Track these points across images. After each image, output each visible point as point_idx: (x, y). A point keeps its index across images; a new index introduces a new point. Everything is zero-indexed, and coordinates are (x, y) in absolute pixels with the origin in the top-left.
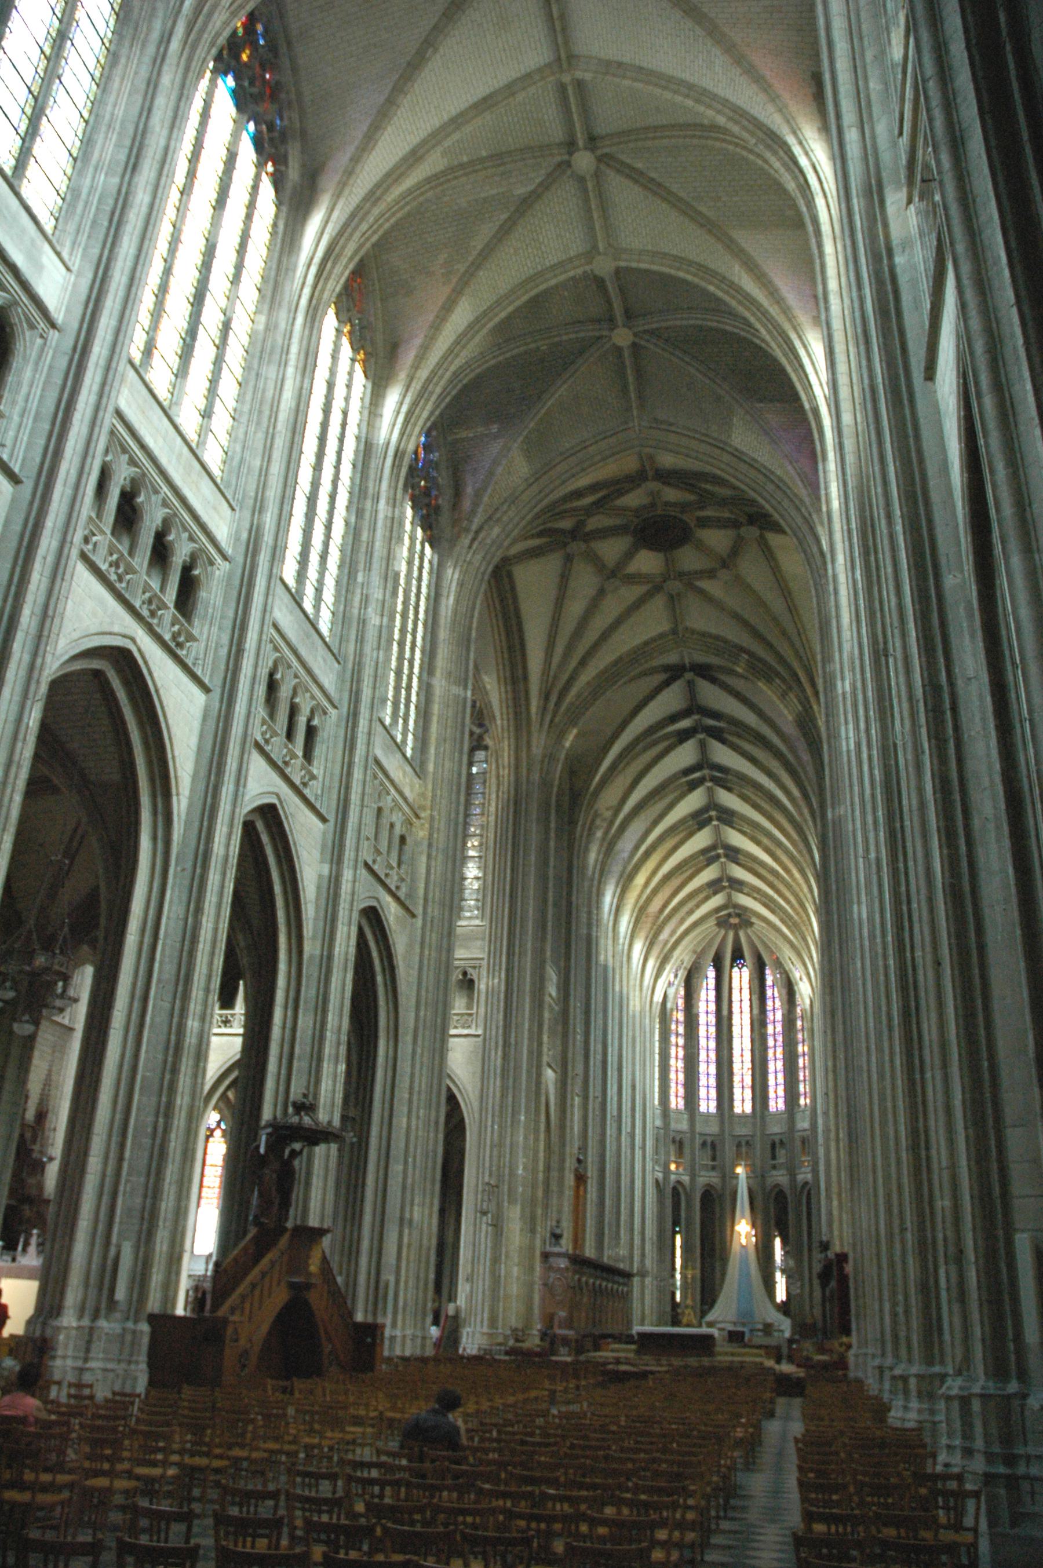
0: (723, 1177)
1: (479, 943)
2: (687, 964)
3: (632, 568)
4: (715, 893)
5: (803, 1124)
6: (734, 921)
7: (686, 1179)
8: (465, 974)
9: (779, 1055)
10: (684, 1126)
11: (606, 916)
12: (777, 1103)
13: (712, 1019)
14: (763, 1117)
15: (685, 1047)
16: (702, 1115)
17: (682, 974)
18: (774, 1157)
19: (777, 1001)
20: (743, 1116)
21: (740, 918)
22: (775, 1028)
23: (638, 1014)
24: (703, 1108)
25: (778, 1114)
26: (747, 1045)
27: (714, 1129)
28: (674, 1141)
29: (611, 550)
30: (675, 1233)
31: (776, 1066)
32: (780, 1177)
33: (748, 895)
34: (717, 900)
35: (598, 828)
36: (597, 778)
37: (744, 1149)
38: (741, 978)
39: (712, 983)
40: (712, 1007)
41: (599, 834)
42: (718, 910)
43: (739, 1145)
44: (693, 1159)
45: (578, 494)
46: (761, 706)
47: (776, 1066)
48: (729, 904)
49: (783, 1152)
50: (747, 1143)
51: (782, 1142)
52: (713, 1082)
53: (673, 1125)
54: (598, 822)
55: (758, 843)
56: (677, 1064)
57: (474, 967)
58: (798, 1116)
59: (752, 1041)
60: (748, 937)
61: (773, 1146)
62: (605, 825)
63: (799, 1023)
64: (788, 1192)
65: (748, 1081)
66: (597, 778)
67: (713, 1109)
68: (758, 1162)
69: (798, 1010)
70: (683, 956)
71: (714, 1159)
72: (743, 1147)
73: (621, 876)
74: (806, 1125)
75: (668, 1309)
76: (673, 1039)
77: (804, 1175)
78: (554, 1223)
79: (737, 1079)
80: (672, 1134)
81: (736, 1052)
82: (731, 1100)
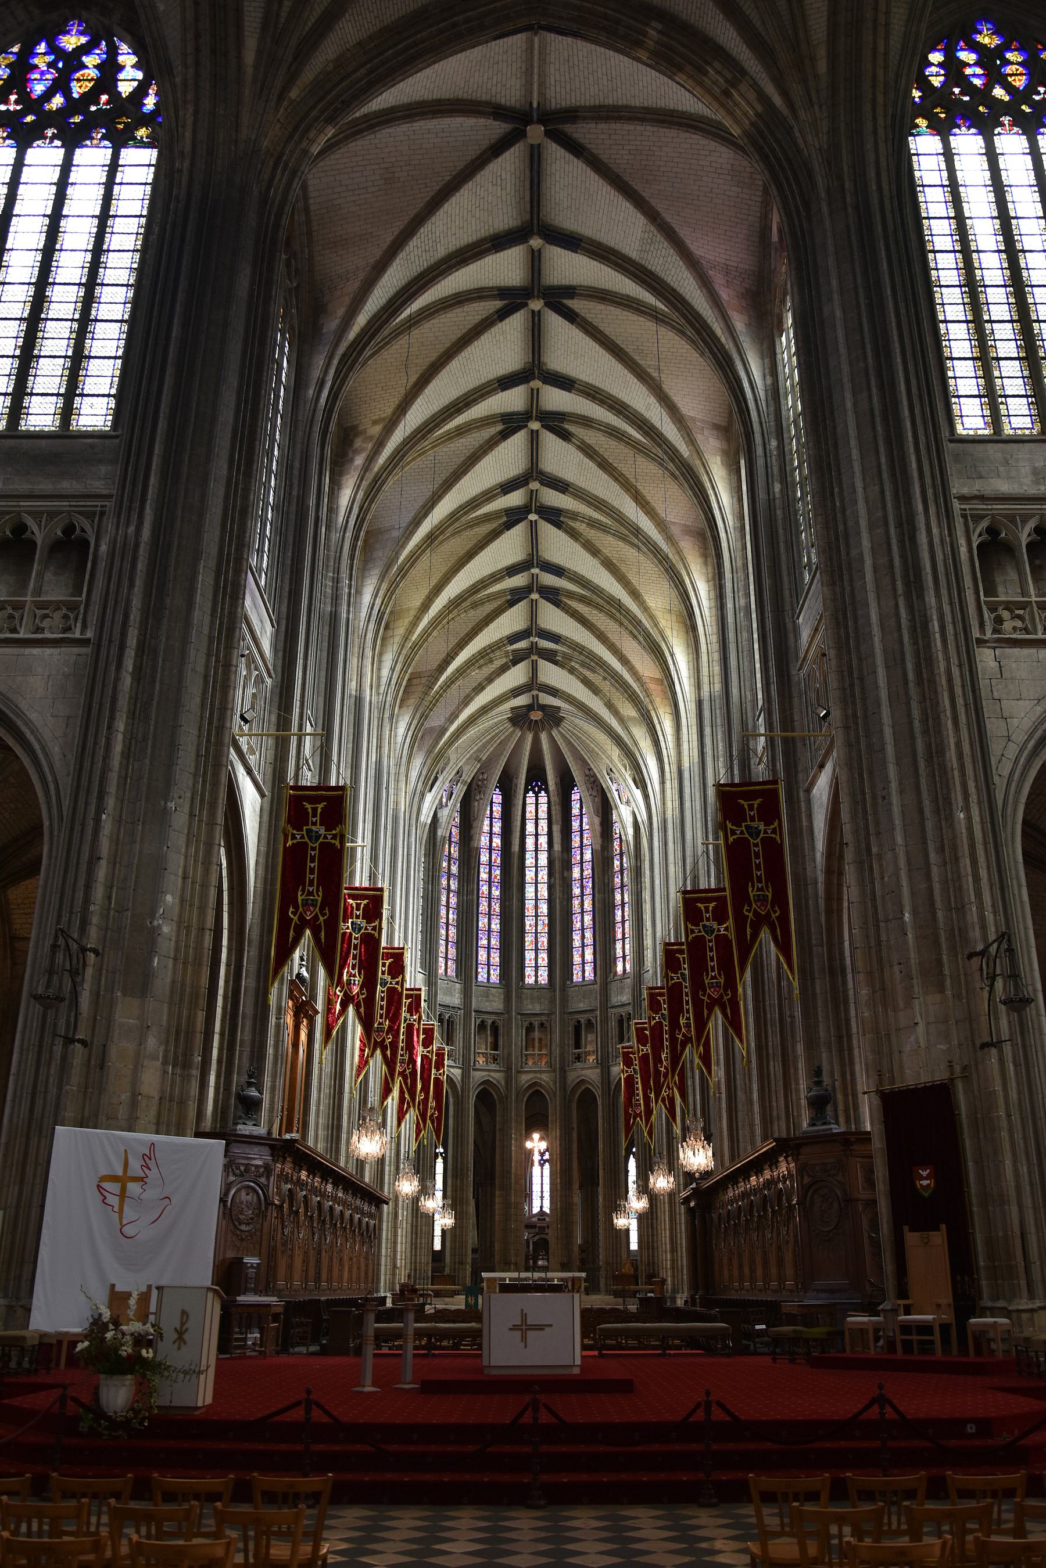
0: (508, 1070)
1: (103, 469)
2: (467, 777)
4: (515, 662)
5: (622, 997)
6: (536, 716)
8: (69, 529)
9: (588, 905)
10: (456, 1000)
14: (564, 988)
15: (459, 893)
17: (460, 791)
18: (578, 1045)
20: (537, 987)
22: (581, 871)
24: (482, 976)
25: (584, 984)
26: (544, 891)
27: (496, 1004)
30: (436, 1156)
31: (583, 920)
32: (589, 1072)
33: (562, 667)
34: (517, 676)
35: (357, 452)
36: (361, 320)
37: (536, 1034)
38: (536, 808)
39: (497, 809)
40: (497, 841)
41: (359, 461)
42: (516, 692)
43: (530, 1029)
44: (467, 1047)
46: (654, 202)
47: (583, 920)
48: (532, 685)
49: (591, 1037)
50: (542, 1025)
52: (495, 942)
53: (441, 998)
54: (358, 443)
55: (593, 550)
56: (448, 915)
57: (89, 515)
58: (614, 987)
60: (553, 741)
62: (370, 446)
63: (617, 863)
64: (598, 1093)
65: (544, 940)
66: (361, 320)
67: (495, 976)
68: (557, 1052)
69: (616, 844)
71: (495, 1047)
74: (625, 998)
75: (425, 1259)
76: (444, 882)
78: (244, 1078)
79: (529, 939)
81: (529, 904)
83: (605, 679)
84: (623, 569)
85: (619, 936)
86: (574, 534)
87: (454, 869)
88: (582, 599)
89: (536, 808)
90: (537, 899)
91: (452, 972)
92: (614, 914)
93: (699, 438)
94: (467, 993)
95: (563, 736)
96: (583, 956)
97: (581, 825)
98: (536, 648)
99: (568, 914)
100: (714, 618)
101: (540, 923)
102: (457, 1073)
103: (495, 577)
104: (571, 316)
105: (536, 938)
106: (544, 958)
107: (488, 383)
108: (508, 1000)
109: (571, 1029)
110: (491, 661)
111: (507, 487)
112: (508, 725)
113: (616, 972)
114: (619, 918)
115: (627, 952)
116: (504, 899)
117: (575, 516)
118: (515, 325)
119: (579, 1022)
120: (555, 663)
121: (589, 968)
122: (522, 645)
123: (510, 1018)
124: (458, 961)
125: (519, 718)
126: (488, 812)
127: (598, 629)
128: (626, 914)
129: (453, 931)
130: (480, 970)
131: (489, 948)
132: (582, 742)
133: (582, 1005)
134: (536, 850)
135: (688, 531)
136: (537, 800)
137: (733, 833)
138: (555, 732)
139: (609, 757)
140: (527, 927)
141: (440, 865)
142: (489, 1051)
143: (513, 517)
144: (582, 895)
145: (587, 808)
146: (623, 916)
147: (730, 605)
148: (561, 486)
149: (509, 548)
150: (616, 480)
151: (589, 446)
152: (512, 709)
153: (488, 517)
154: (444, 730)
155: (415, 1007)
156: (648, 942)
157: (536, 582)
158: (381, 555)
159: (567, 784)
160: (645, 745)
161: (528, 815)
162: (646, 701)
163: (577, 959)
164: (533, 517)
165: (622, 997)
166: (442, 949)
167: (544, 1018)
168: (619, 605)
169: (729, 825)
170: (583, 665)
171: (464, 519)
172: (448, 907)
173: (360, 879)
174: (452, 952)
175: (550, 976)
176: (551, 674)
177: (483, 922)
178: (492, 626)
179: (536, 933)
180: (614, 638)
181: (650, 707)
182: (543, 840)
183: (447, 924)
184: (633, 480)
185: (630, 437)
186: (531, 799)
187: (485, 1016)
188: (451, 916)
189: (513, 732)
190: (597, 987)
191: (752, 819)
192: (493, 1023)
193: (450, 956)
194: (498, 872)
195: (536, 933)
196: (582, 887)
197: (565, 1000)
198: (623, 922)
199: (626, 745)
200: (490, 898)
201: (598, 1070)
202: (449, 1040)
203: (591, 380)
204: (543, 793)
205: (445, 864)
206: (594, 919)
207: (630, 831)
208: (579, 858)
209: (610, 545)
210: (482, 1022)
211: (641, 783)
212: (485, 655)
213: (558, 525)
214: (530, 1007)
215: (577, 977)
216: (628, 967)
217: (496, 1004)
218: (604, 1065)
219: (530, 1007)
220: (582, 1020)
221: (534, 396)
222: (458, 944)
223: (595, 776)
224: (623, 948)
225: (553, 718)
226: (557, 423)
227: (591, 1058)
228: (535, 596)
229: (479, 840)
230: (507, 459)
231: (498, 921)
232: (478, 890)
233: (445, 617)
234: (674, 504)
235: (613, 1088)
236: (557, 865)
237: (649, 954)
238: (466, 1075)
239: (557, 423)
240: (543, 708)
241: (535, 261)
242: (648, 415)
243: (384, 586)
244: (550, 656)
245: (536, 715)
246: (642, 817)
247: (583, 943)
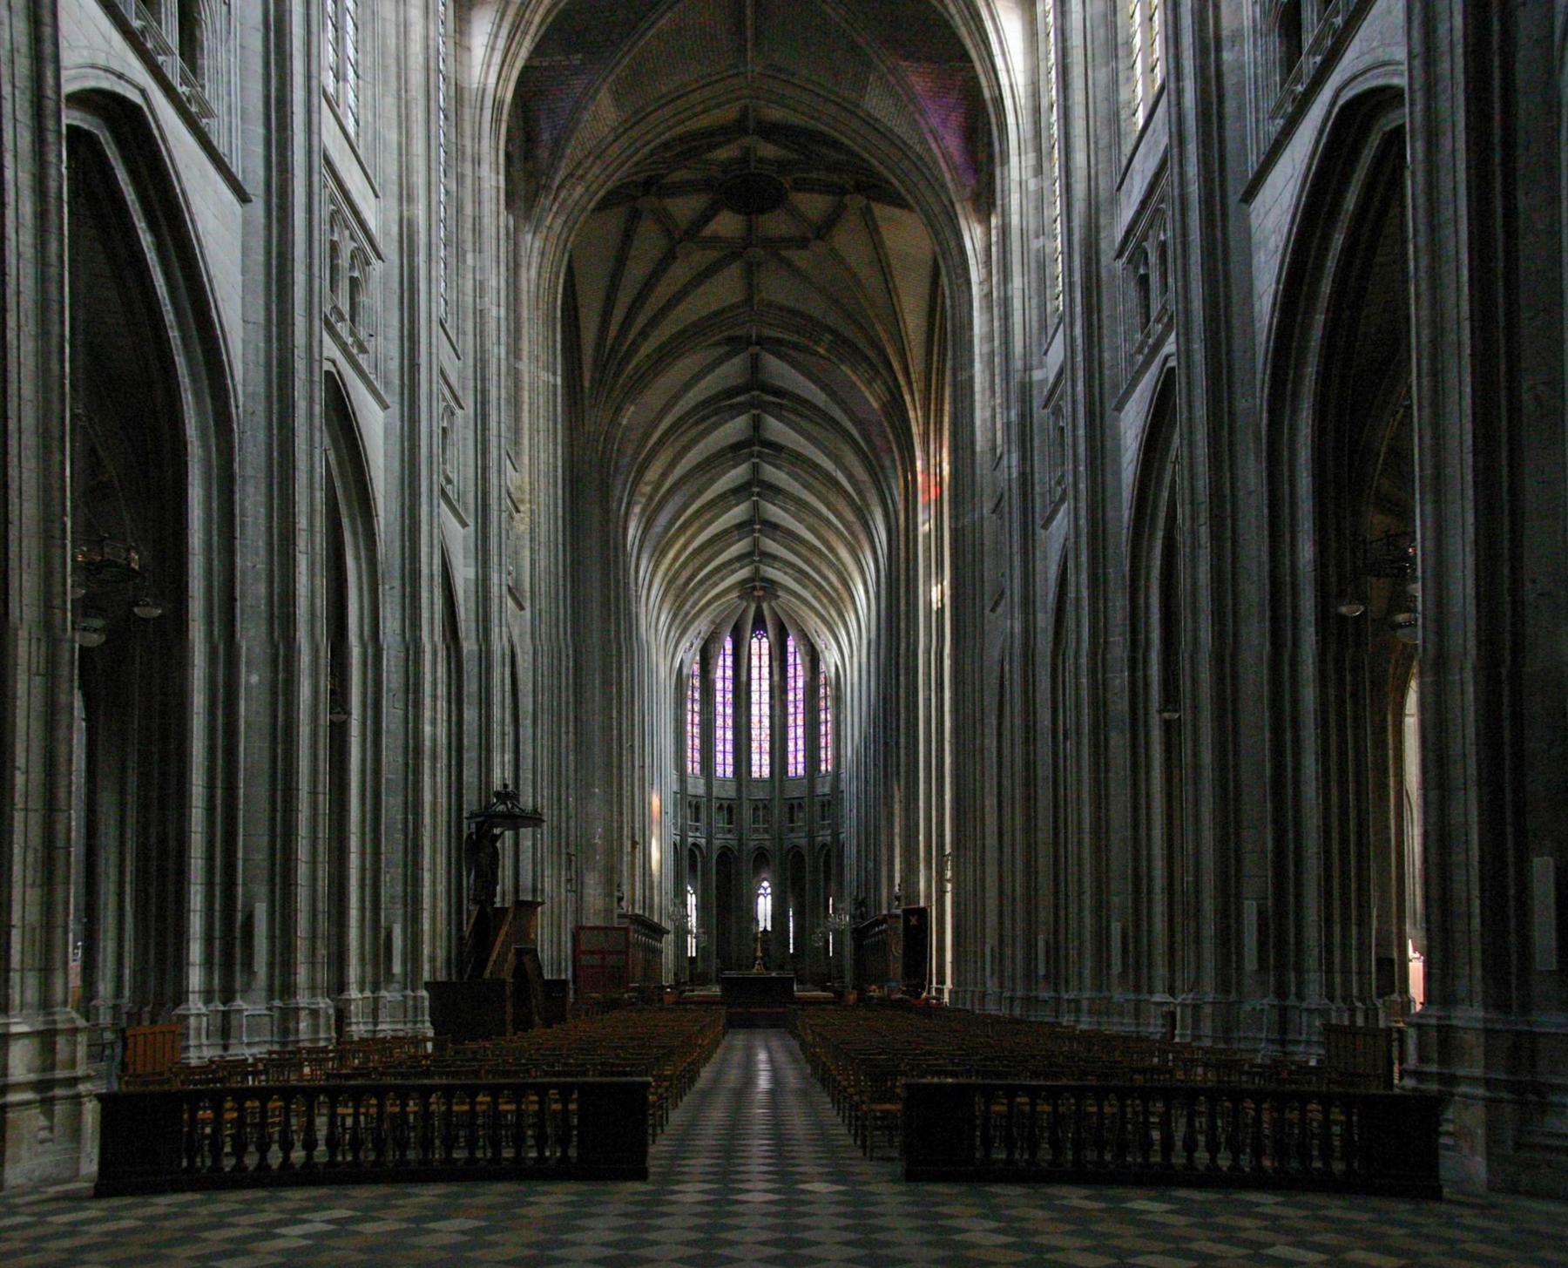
0: (740, 840)
3: (708, 231)
10: (701, 791)
13: (729, 685)
15: (701, 713)
16: (718, 779)
17: (698, 644)
18: (792, 821)
20: (761, 780)
21: (771, 587)
26: (766, 710)
27: (732, 793)
29: (684, 208)
40: (729, 673)
43: (756, 809)
44: (709, 824)
45: (666, 146)
52: (729, 747)
53: (691, 790)
56: (693, 731)
61: (792, 808)
64: (805, 852)
67: (729, 771)
70: (702, 626)
71: (730, 822)
77: (824, 836)
81: (755, 719)
82: (750, 765)
87: (697, 695)
94: (709, 785)
106: (766, 759)
124: (702, 763)
129: (697, 741)
157: (756, 524)
174: (697, 756)
177: (719, 733)
197: (782, 791)
217: (732, 793)
222: (702, 751)
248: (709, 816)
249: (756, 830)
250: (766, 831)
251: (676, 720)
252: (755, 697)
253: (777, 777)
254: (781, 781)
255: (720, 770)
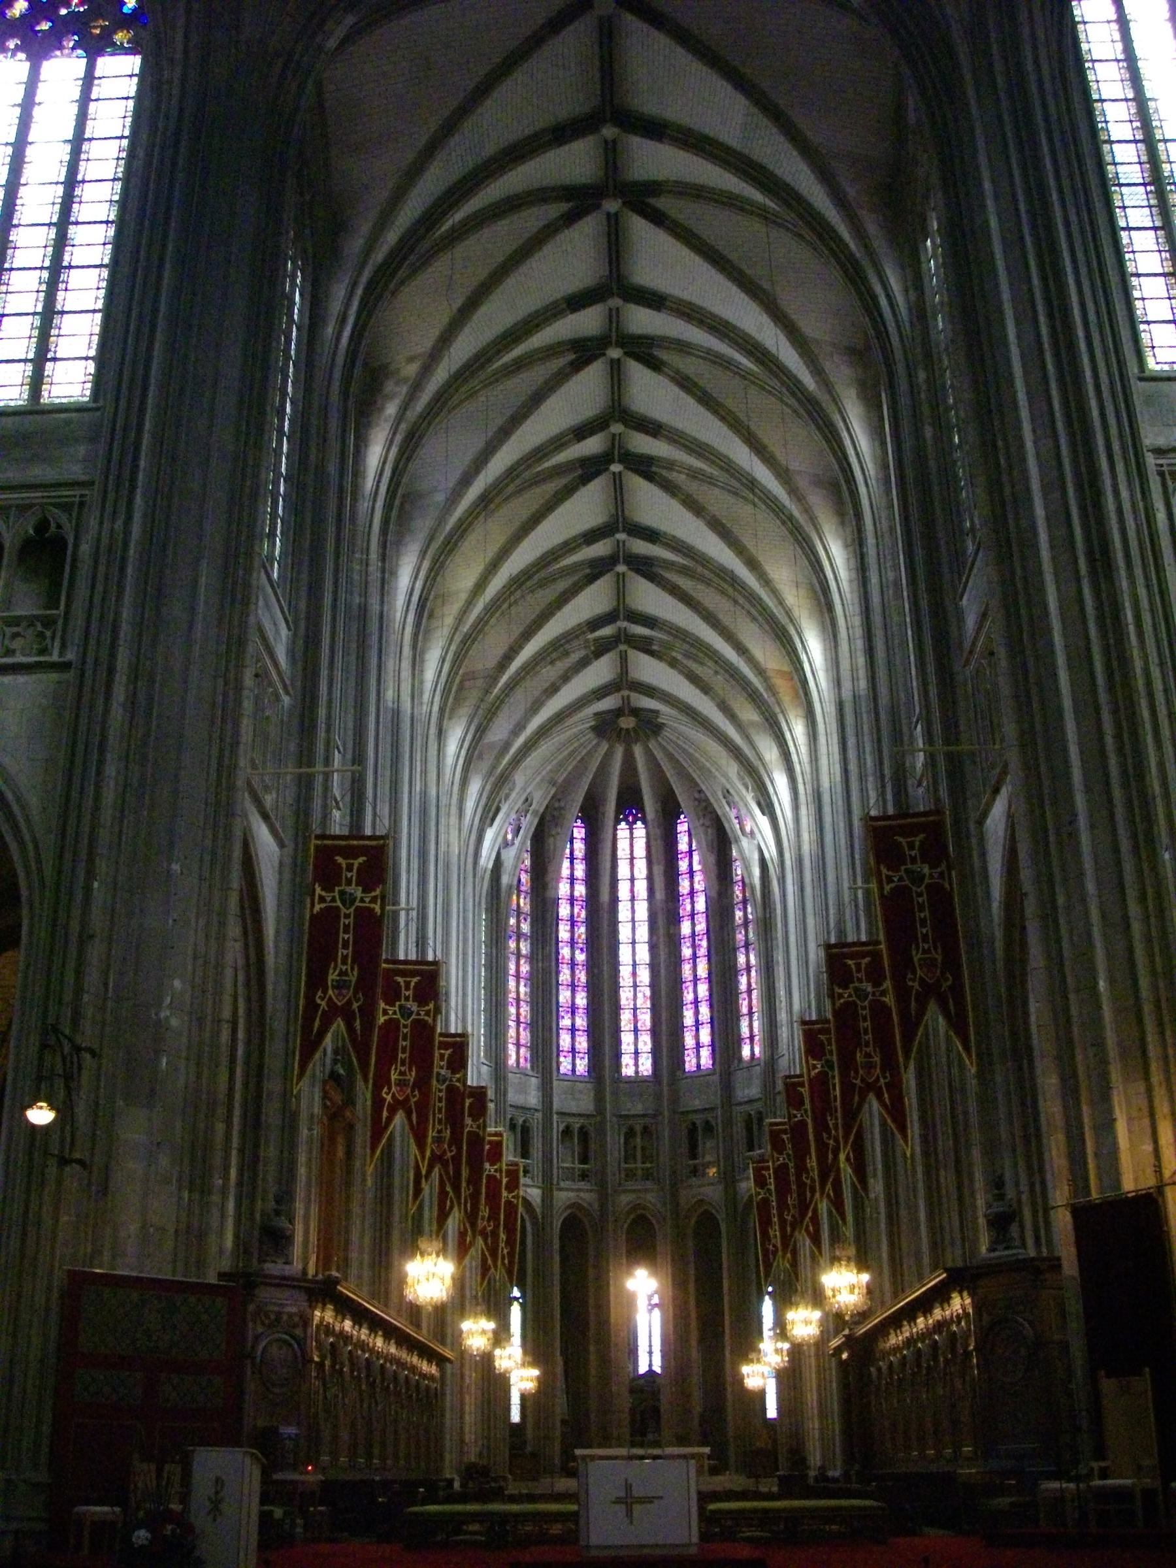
4: (598, 654)
5: (749, 1089)
6: (627, 723)
7: (534, 1194)
9: (702, 969)
10: (533, 1099)
11: (398, 615)
12: (698, 1053)
14: (673, 1081)
15: (532, 959)
16: (564, 1079)
17: (529, 823)
18: (693, 1155)
19: (698, 877)
22: (693, 925)
23: (454, 860)
26: (643, 954)
27: (585, 1103)
28: (513, 1127)
32: (708, 1186)
34: (600, 671)
39: (579, 847)
40: (580, 890)
42: (600, 693)
43: (630, 1134)
44: (547, 1158)
47: (697, 990)
48: (623, 682)
50: (646, 1130)
51: (709, 1128)
52: (581, 1022)
53: (513, 1097)
56: (518, 989)
58: (739, 1077)
59: (653, 948)
61: (693, 1130)
63: (739, 914)
65: (645, 1019)
67: (582, 1066)
69: (738, 891)
71: (584, 1159)
72: (640, 1134)
73: (431, 539)
74: (754, 1091)
76: (512, 945)
79: (626, 1017)
80: (510, 1113)
81: (625, 972)
82: (617, 1055)
83: (716, 673)
84: (736, 529)
85: (745, 1010)
86: (669, 487)
87: (525, 927)
88: (684, 571)
89: (631, 843)
90: (634, 965)
91: (526, 1065)
92: (737, 982)
93: (827, 366)
95: (664, 749)
96: (697, 1037)
97: (691, 865)
98: (626, 635)
99: (677, 983)
100: (856, 595)
101: (640, 995)
102: (534, 1194)
103: (568, 547)
104: (658, 219)
105: (635, 1016)
107: (555, 304)
108: (599, 1099)
109: (685, 1133)
110: (567, 654)
111: (581, 432)
112: (591, 735)
113: (740, 1058)
114: (743, 986)
115: (756, 1031)
116: (592, 966)
117: (670, 465)
118: (588, 229)
119: (694, 1124)
120: (652, 653)
121: (705, 1053)
122: (607, 631)
123: (603, 1122)
124: (533, 1048)
125: (605, 726)
126: (568, 851)
127: (705, 609)
128: (753, 980)
129: (525, 1010)
130: (562, 1059)
131: (573, 1030)
132: (690, 756)
133: (697, 1102)
134: (633, 899)
135: (817, 482)
136: (631, 834)
137: (890, 880)
138: (652, 744)
139: (726, 776)
140: (623, 1002)
141: (507, 919)
142: (578, 1166)
143: (590, 469)
144: (695, 957)
145: (698, 842)
146: (749, 984)
147: (874, 579)
148: (653, 428)
149: (585, 508)
150: (723, 419)
151: (687, 378)
152: (596, 714)
153: (559, 470)
154: (507, 746)
155: (479, 1110)
156: (782, 1016)
158: (422, 526)
159: (670, 813)
160: (770, 753)
161: (620, 854)
162: (771, 700)
163: (689, 1041)
164: (616, 468)
165: (749, 1089)
166: (512, 1032)
167: (647, 1120)
168: (734, 580)
169: (884, 871)
170: (687, 655)
171: (527, 475)
172: (518, 976)
173: (406, 950)
175: (655, 1064)
176: (648, 669)
177: (564, 996)
178: (568, 608)
179: (635, 1009)
180: (726, 620)
181: (777, 710)
182: (641, 887)
183: (518, 1000)
184: (744, 419)
185: (738, 365)
186: (623, 831)
187: (571, 1120)
188: (522, 989)
189: (598, 745)
190: (716, 1078)
191: (913, 860)
192: (582, 1128)
193: (522, 1041)
194: (583, 929)
195: (635, 1009)
196: (694, 946)
198: (749, 991)
199: (747, 760)
200: (573, 964)
201: (721, 1187)
202: (525, 1154)
203: (685, 296)
204: (639, 824)
205: (512, 921)
206: (710, 990)
207: (756, 872)
208: (689, 907)
209: (717, 500)
210: (567, 1127)
211: (767, 807)
212: (558, 647)
213: (649, 477)
214: (629, 1105)
215: (690, 1064)
216: (757, 1050)
217: (585, 1103)
218: (729, 1179)
219: (629, 1105)
220: (698, 1122)
221: (614, 317)
222: (533, 1026)
223: (707, 800)
224: (750, 1026)
225: (650, 725)
226: (645, 350)
227: (712, 1171)
228: (621, 568)
229: (557, 888)
230: (584, 394)
231: (584, 994)
232: (558, 953)
233: (504, 601)
234: (799, 448)
235: (740, 1208)
236: (661, 921)
237: (784, 1033)
238: (547, 1197)
239: (645, 350)
240: (636, 712)
241: (611, 151)
242: (759, 337)
243: (426, 564)
244: (645, 646)
245: (627, 722)
246: (771, 852)
247: (697, 1021)
248: (547, 1141)
249: (630, 1175)
250: (647, 1175)
251: (489, 966)
252: (624, 932)
253: (665, 1073)
254: (673, 1081)
255: (565, 1065)
